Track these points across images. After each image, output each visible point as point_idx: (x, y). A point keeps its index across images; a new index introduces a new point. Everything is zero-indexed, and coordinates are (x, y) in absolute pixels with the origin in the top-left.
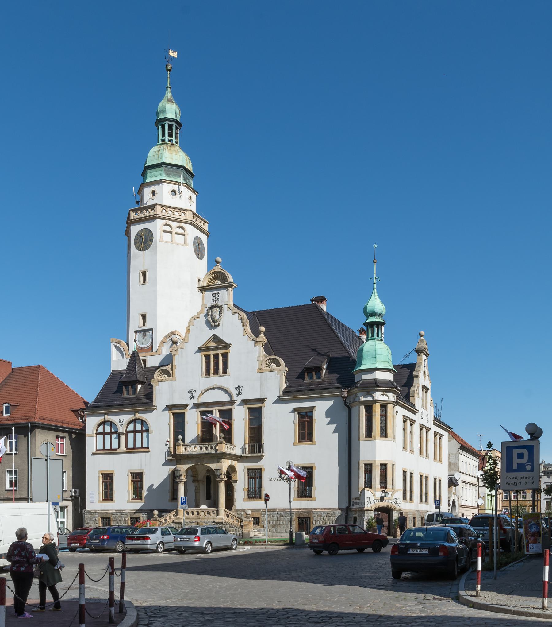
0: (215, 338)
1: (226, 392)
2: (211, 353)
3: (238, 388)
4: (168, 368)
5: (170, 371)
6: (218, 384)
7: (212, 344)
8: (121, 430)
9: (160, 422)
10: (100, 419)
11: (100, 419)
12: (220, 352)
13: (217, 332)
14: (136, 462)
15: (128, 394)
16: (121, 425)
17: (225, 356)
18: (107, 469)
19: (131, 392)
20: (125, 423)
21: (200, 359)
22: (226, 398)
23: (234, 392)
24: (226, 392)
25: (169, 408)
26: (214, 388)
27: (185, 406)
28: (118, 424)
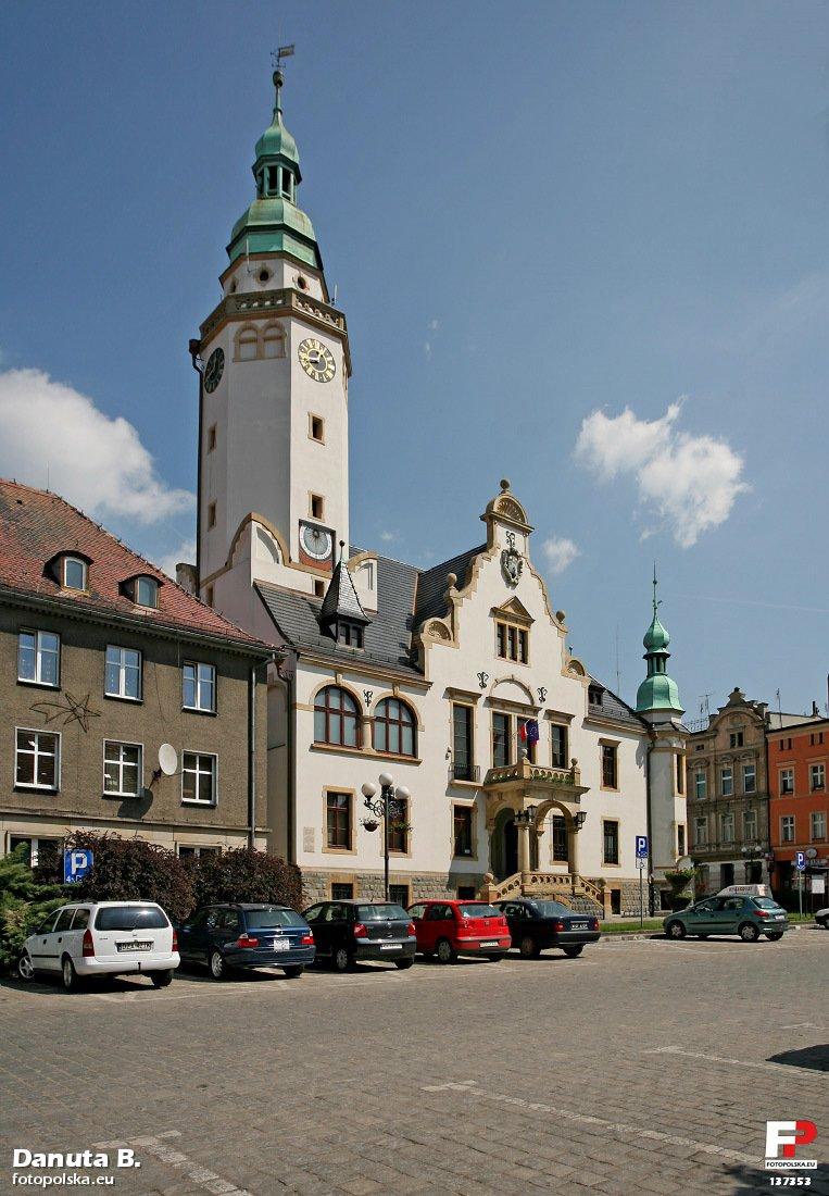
0: (516, 602)
1: (527, 691)
2: (508, 623)
3: (541, 690)
4: (446, 621)
5: (450, 630)
6: (517, 678)
7: (510, 610)
8: (368, 711)
9: (435, 716)
10: (326, 679)
11: (326, 679)
12: (519, 627)
13: (519, 592)
14: (402, 778)
15: (348, 643)
16: (368, 702)
17: (524, 634)
18: (341, 785)
19: (354, 642)
20: (374, 699)
21: (491, 626)
22: (526, 701)
23: (536, 696)
24: (527, 691)
25: (451, 692)
26: (512, 681)
27: (475, 697)
28: (362, 699)
